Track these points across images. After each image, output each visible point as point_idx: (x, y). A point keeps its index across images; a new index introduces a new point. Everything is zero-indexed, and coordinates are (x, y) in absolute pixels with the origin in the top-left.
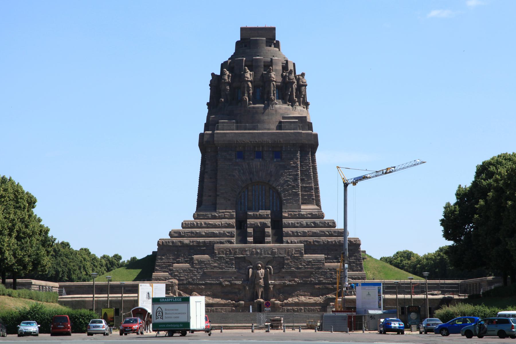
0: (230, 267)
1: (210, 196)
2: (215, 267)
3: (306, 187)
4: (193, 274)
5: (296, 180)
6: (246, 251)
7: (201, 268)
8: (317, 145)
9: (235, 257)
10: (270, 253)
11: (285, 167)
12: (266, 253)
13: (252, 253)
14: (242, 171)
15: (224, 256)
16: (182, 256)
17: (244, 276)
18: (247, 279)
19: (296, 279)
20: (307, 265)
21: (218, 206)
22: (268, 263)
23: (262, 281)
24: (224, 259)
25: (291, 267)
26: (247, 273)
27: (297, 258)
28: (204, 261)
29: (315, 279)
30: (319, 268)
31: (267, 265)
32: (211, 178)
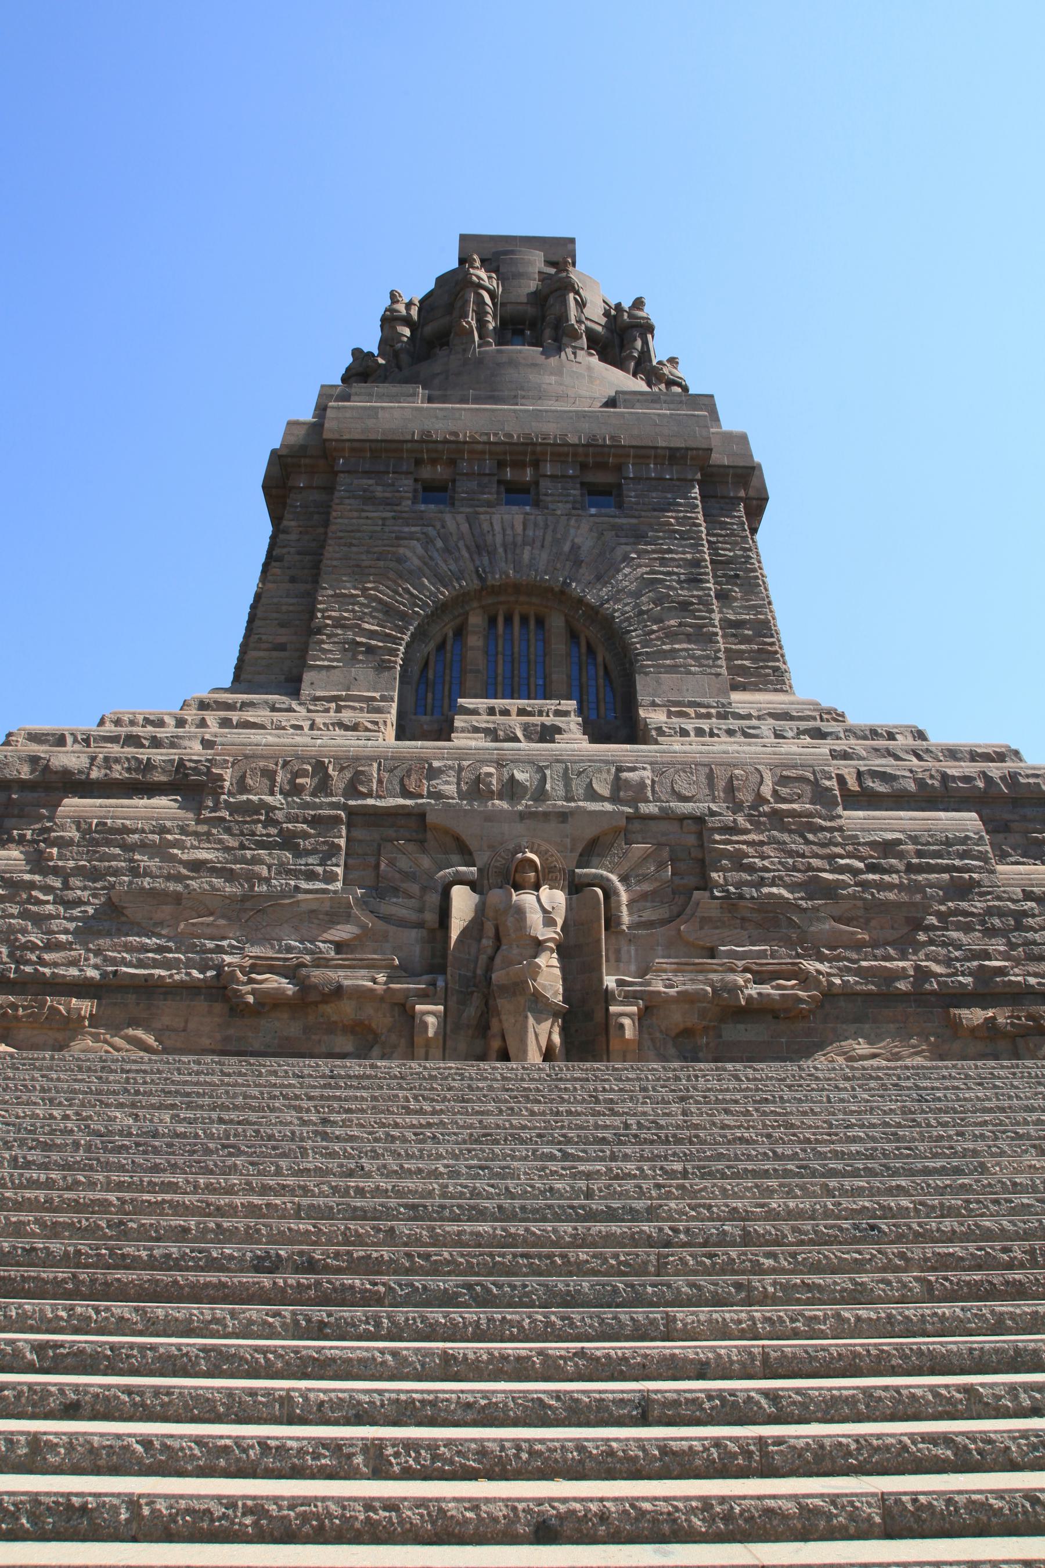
0: (311, 876)
1: (282, 647)
2: (197, 866)
3: (739, 624)
4: (24, 915)
5: (695, 581)
6: (433, 773)
7: (94, 875)
8: (767, 499)
9: (351, 812)
10: (603, 789)
11: (638, 536)
12: (578, 790)
13: (477, 789)
14: (439, 544)
15: (276, 800)
16: (21, 841)
17: (413, 934)
18: (434, 959)
19: (811, 966)
20: (872, 868)
21: (308, 677)
22: (592, 850)
23: (549, 975)
24: (270, 822)
25: (762, 883)
26: (431, 917)
27: (804, 827)
28: (126, 830)
29: (948, 962)
30: (963, 890)
31: (584, 861)
32: (293, 580)
